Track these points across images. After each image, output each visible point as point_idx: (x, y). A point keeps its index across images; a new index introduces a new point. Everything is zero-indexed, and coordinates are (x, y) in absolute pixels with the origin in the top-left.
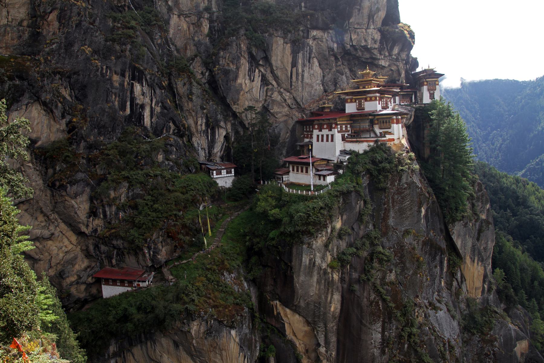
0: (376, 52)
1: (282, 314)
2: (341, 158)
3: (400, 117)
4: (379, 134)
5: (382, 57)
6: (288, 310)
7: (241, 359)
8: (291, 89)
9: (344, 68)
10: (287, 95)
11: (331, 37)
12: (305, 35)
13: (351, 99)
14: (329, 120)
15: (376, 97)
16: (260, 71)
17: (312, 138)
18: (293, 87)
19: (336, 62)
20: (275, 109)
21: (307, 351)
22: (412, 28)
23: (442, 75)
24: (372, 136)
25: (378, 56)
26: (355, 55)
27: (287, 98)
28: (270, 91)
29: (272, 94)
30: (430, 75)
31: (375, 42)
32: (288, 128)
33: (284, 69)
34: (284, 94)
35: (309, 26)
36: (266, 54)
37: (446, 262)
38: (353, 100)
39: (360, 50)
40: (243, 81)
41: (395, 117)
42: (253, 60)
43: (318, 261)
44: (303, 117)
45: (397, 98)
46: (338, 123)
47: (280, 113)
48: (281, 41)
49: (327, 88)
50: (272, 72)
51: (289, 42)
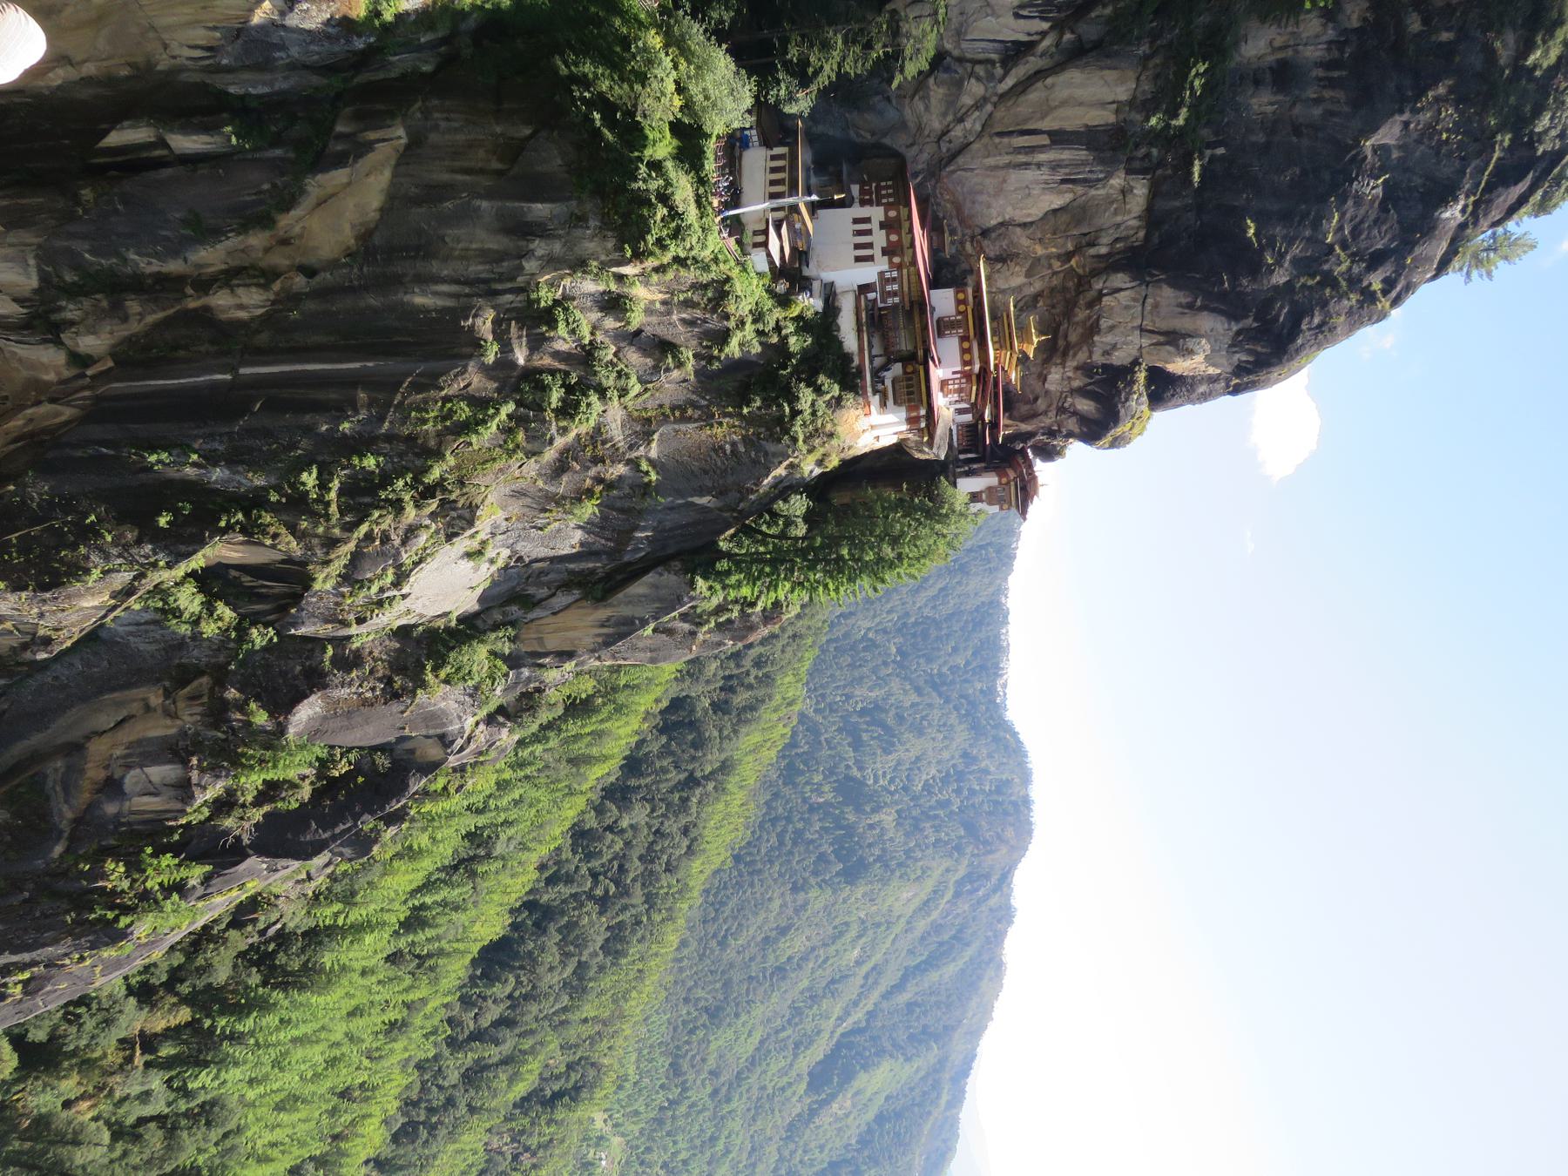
0: (1082, 356)
1: (371, 158)
2: (816, 286)
3: (923, 425)
5: (1070, 374)
6: (387, 174)
7: (200, 36)
8: (991, 136)
10: (973, 123)
11: (1126, 238)
12: (1137, 165)
14: (912, 245)
16: (1043, 34)
18: (997, 140)
19: (1058, 257)
20: (937, 93)
21: (285, 242)
25: (1071, 364)
26: (1075, 304)
27: (968, 124)
28: (987, 71)
29: (978, 79)
30: (1024, 489)
31: (1106, 353)
32: (885, 135)
33: (1046, 110)
34: (977, 114)
35: (1159, 172)
36: (1091, 50)
37: (591, 565)
38: (962, 308)
39: (1089, 317)
41: (923, 412)
43: (540, 247)
44: (915, 175)
47: (927, 108)
48: (1123, 93)
50: (1039, 75)
51: (1121, 117)
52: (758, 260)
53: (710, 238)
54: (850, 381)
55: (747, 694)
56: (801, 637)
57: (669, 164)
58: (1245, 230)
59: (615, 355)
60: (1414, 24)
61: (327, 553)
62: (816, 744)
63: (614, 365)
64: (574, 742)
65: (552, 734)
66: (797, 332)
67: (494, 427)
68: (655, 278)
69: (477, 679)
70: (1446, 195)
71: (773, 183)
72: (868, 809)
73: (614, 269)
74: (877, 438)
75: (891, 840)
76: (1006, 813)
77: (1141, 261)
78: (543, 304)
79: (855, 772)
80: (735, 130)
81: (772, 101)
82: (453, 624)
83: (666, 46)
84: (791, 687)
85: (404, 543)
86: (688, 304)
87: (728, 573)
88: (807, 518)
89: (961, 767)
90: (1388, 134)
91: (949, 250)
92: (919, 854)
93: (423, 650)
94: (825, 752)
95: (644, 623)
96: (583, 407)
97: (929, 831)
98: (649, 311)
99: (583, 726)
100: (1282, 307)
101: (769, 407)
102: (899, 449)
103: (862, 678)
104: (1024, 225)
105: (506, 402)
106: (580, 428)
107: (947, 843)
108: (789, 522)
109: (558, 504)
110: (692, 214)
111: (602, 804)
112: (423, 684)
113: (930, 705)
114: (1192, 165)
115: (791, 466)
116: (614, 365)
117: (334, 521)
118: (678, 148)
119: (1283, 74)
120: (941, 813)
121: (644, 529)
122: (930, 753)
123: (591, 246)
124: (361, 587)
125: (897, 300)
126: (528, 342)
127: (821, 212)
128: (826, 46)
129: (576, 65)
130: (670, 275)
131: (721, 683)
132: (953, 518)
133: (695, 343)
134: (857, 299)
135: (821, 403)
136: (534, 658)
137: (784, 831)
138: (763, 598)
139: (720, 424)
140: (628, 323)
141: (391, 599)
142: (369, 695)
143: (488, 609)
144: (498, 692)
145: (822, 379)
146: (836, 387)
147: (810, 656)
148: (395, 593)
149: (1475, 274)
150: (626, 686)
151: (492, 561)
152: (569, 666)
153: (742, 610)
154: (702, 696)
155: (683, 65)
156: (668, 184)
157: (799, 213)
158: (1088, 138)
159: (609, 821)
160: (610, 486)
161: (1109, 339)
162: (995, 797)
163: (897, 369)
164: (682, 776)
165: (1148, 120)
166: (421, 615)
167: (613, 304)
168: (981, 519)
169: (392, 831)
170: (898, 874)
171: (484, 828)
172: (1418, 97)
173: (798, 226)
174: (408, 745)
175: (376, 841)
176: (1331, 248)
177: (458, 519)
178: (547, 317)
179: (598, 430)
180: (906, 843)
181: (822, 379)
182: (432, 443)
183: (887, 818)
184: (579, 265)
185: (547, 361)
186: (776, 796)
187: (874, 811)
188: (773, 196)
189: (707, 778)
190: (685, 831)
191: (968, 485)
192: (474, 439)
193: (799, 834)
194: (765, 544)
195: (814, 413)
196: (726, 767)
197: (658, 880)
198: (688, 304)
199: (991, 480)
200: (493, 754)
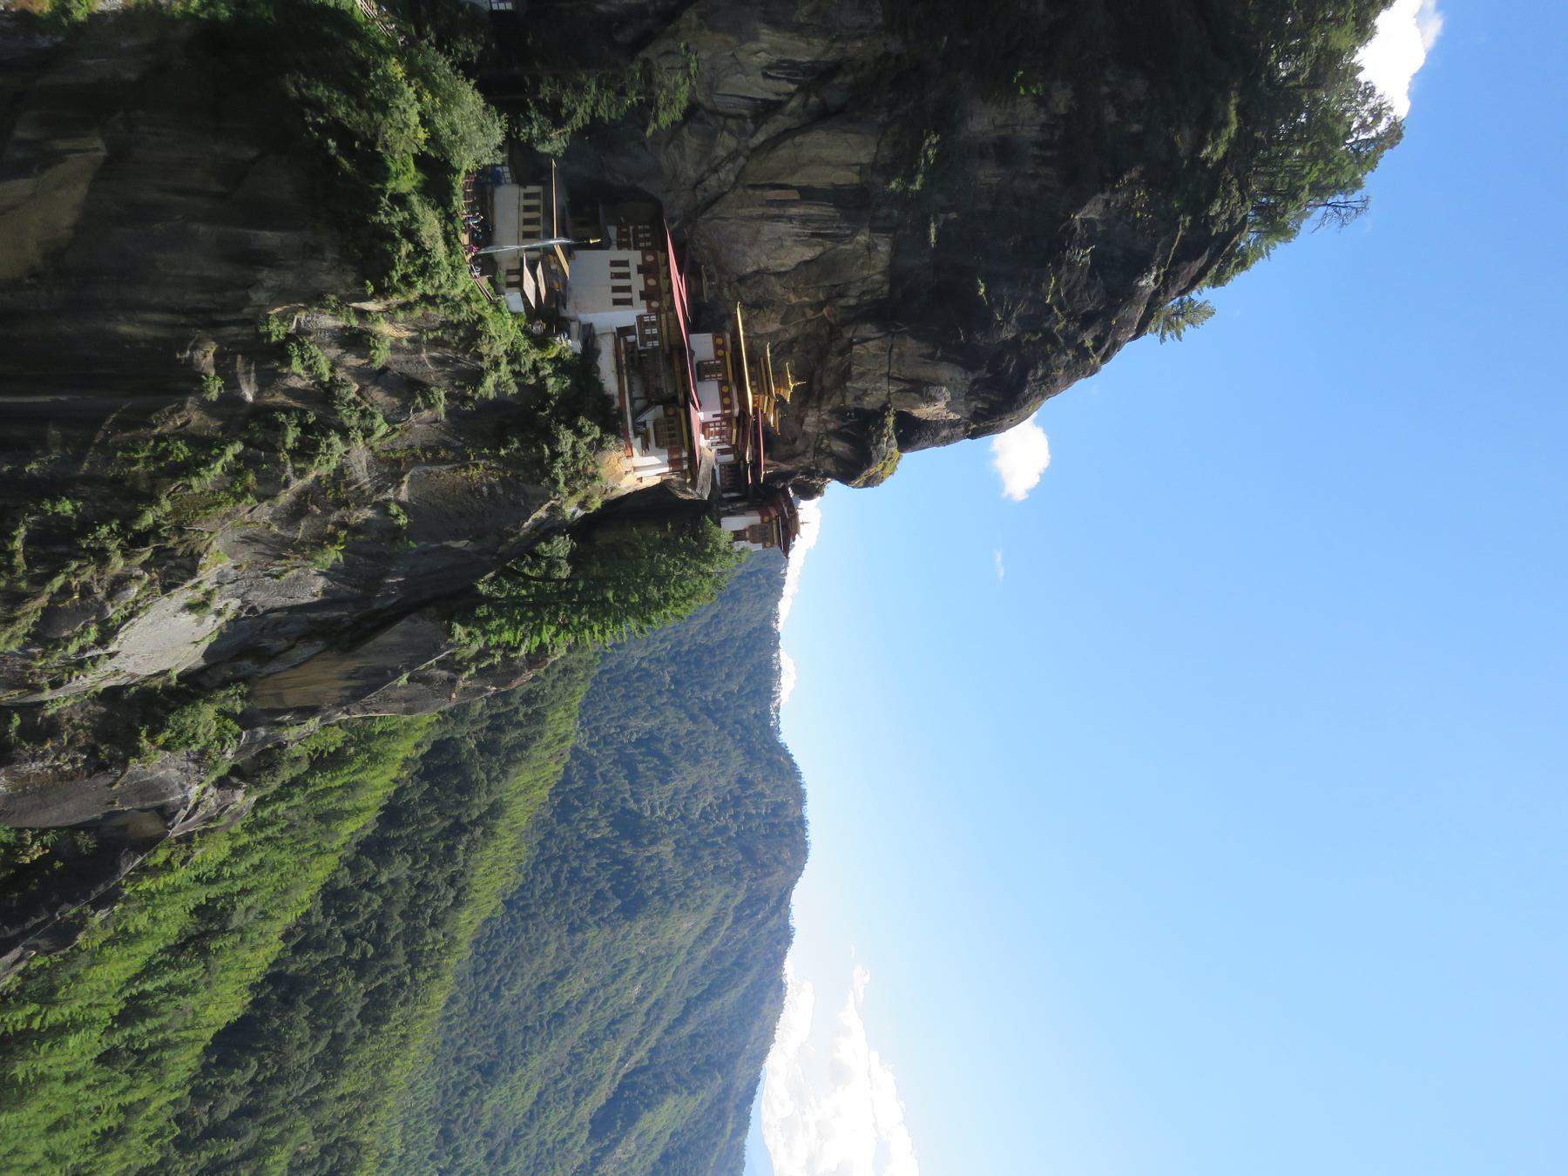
0: (836, 400)
2: (574, 327)
3: (685, 467)
4: (642, 419)
9: (797, 325)
10: (727, 174)
11: (872, 291)
15: (730, 406)
16: (791, 95)
18: (750, 192)
19: (811, 306)
20: (691, 142)
22: (889, 484)
27: (722, 175)
29: (731, 133)
30: (785, 527)
37: (335, 614)
38: (721, 353)
40: (765, 46)
41: (685, 454)
42: (817, 76)
43: (269, 278)
44: (672, 220)
47: (682, 156)
48: (864, 157)
49: (749, 282)
50: (788, 133)
52: (512, 300)
53: (460, 277)
54: (612, 425)
55: (515, 734)
56: (572, 671)
57: (414, 199)
58: (977, 288)
59: (359, 393)
60: (1110, 115)
61: (12, 610)
62: (591, 779)
63: (357, 404)
64: (323, 797)
65: (297, 790)
66: (555, 374)
67: (219, 470)
68: (401, 315)
69: (203, 742)
70: (1141, 268)
71: (527, 222)
72: (645, 841)
73: (355, 305)
74: (640, 479)
75: (670, 870)
76: (782, 835)
77: (886, 312)
78: (274, 339)
79: (632, 805)
80: (485, 167)
81: (524, 138)
82: (173, 683)
83: (409, 76)
84: (563, 723)
85: (110, 595)
86: (437, 343)
87: (489, 618)
88: (572, 558)
89: (737, 792)
90: (1091, 211)
91: (707, 296)
92: (698, 883)
93: (141, 711)
94: (600, 786)
95: (397, 673)
96: (323, 448)
97: (707, 859)
98: (395, 348)
99: (333, 779)
100: (1010, 361)
101: (528, 448)
102: (662, 488)
103: (636, 709)
104: (779, 275)
105: (232, 442)
106: (320, 469)
107: (725, 869)
108: (552, 564)
109: (296, 550)
110: (441, 250)
111: (357, 860)
112: (137, 752)
113: (706, 733)
114: (928, 227)
115: (552, 509)
116: (359, 404)
117: (20, 572)
118: (425, 182)
119: (1004, 151)
120: (719, 840)
121: (395, 575)
122: (707, 780)
123: (328, 279)
124: (57, 647)
125: (656, 343)
126: (258, 377)
127: (579, 254)
128: (579, 89)
129: (308, 87)
130: (418, 312)
131: (485, 724)
132: (718, 557)
133: (446, 382)
135: (582, 445)
136: (271, 716)
137: (560, 871)
138: (527, 642)
139: (476, 466)
140: (372, 361)
141: (94, 660)
142: (68, 768)
143: (215, 664)
144: (229, 755)
145: (582, 421)
146: (597, 429)
147: (581, 690)
148: (100, 651)
149: (1168, 336)
150: (382, 733)
151: (219, 613)
152: (313, 724)
153: (505, 656)
154: (468, 738)
155: (427, 97)
156: (414, 219)
157: (555, 254)
158: (834, 195)
159: (366, 878)
160: (355, 530)
161: (860, 385)
162: (771, 820)
163: (657, 412)
164: (447, 824)
165: (888, 182)
166: (133, 676)
167: (356, 341)
168: (744, 557)
169: (101, 915)
170: (677, 905)
171: (217, 899)
172: (1116, 180)
173: (553, 267)
174: (118, 821)
175: (80, 928)
176: (1050, 307)
177: (175, 568)
178: (280, 352)
179: (340, 471)
180: (685, 873)
181: (582, 421)
182: (143, 486)
183: (666, 849)
184: (316, 299)
185: (280, 398)
186: (550, 835)
187: (653, 842)
188: (528, 236)
189: (474, 823)
190: (451, 881)
191: (732, 524)
192: (195, 481)
193: (574, 872)
194: (526, 586)
195: (575, 455)
196: (496, 810)
197: (422, 936)
198: (437, 343)
200: (225, 819)
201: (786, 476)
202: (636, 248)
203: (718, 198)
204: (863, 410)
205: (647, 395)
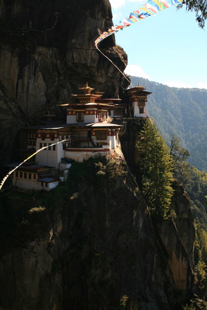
3: (114, 130)
4: (96, 144)
13: (72, 112)
15: (94, 111)
17: (36, 145)
18: (18, 97)
22: (127, 51)
23: (151, 93)
24: (89, 146)
27: (13, 106)
38: (74, 113)
41: (110, 130)
45: (112, 112)
46: (60, 133)
71: (25, 177)
134: (68, 150)
158: (21, 67)
161: (89, 61)
199: (136, 104)
201: (120, 89)
202: (36, 140)
203: (19, 108)
204: (98, 60)
205: (87, 141)
